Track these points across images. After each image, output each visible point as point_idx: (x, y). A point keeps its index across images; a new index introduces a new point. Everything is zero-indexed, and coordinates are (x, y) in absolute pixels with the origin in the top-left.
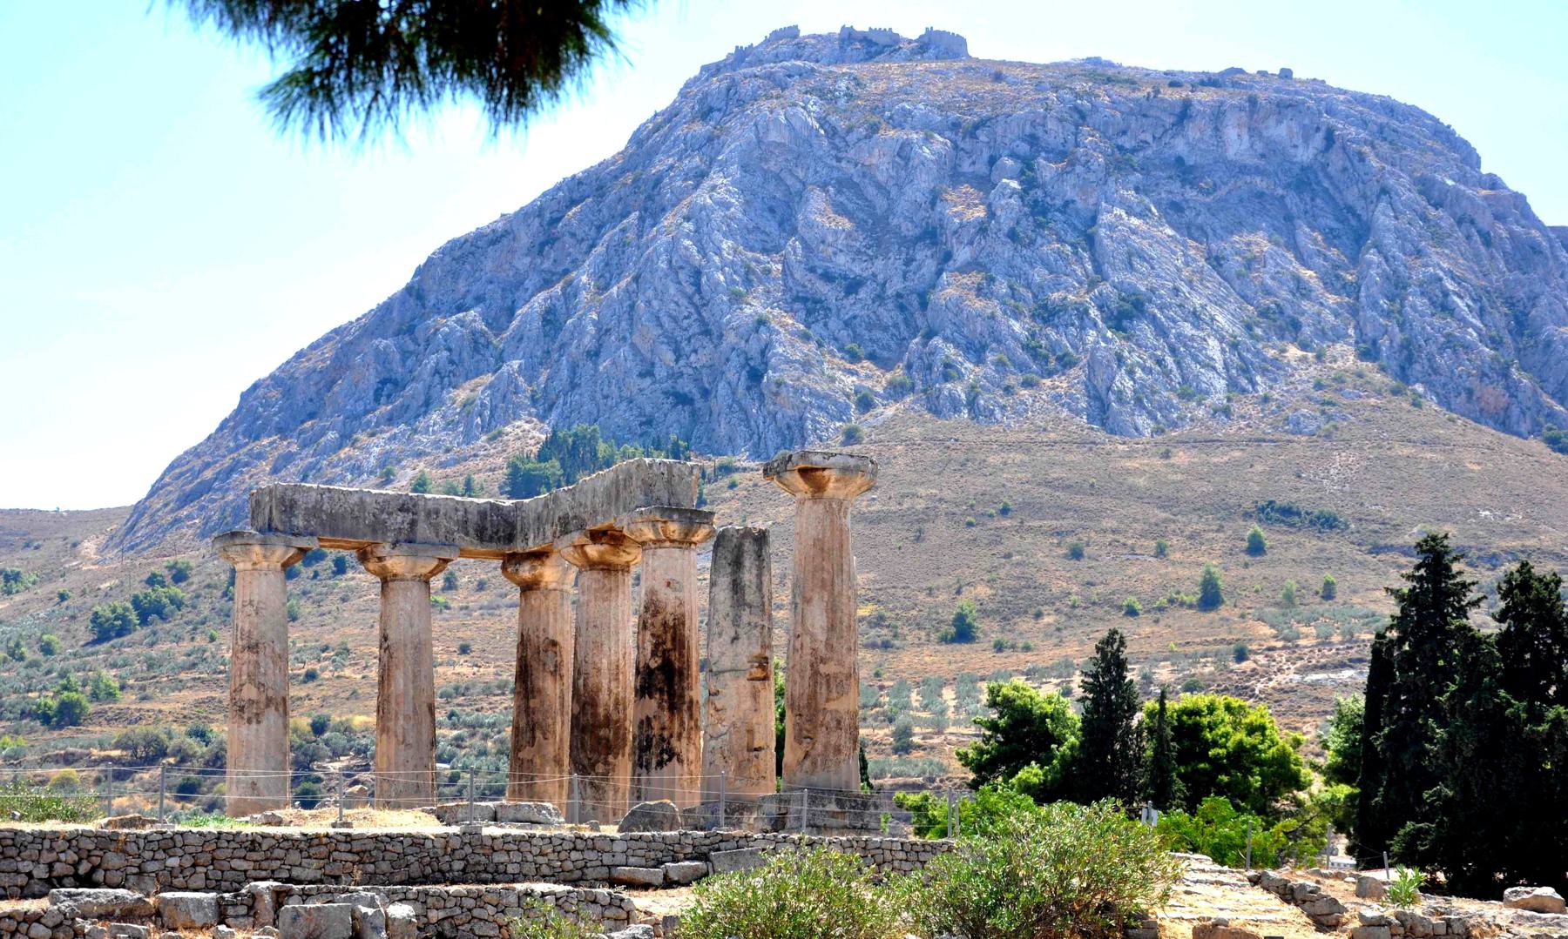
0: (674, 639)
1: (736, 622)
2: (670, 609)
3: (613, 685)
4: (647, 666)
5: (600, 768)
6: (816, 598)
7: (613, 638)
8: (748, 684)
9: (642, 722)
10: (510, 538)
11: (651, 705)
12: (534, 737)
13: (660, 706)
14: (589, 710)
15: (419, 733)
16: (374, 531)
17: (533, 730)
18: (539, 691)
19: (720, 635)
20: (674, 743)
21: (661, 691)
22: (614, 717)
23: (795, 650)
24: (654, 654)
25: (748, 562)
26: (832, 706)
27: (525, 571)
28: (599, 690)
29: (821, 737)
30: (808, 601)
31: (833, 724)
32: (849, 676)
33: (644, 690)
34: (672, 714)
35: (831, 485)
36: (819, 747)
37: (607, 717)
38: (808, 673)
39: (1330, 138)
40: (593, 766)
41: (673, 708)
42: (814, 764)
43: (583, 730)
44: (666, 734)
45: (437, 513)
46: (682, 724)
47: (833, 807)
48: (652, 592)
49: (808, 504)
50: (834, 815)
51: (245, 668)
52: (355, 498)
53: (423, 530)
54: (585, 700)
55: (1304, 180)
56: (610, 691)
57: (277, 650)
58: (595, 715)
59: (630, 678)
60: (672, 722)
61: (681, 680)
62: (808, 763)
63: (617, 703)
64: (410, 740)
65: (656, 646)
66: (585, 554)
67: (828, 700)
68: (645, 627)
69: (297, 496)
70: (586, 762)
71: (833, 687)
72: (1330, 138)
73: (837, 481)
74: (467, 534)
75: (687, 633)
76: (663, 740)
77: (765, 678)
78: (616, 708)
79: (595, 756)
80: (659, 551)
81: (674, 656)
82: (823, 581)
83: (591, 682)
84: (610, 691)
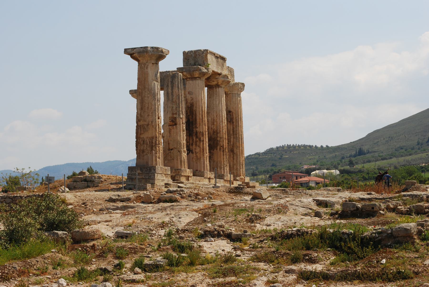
22: (213, 137)
31: (142, 142)
32: (148, 125)
46: (193, 140)
56: (211, 128)
60: (190, 140)
63: (214, 132)
78: (213, 134)
84: (211, 128)
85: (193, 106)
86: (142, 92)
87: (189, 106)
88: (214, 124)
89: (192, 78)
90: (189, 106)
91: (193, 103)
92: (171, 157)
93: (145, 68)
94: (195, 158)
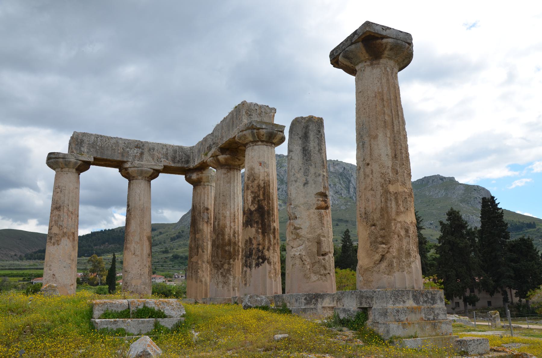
0: (264, 194)
1: (306, 173)
2: (261, 178)
3: (232, 224)
4: (250, 210)
5: (226, 266)
6: (381, 135)
7: (232, 202)
8: (316, 211)
9: (247, 241)
10: (188, 162)
11: (252, 231)
12: (198, 252)
13: (257, 231)
14: (221, 237)
15: (142, 250)
16: (123, 156)
17: (198, 248)
18: (200, 230)
19: (296, 181)
20: (266, 253)
21: (257, 223)
22: (233, 240)
23: (366, 176)
24: (253, 202)
25: (312, 135)
26: (399, 219)
27: (194, 176)
28: (225, 227)
29: (395, 243)
30: (376, 137)
31: (403, 233)
33: (248, 223)
34: (264, 236)
35: (386, 53)
36: (394, 252)
37: (230, 240)
38: (380, 191)
39: (344, 168)
40: (222, 265)
41: (263, 233)
42: (390, 265)
43: (218, 247)
44: (261, 247)
45: (154, 149)
47: (411, 303)
48: (252, 169)
49: (368, 69)
50: (412, 310)
51: (54, 218)
52: (114, 141)
53: (146, 156)
54: (219, 232)
55: (341, 174)
56: (231, 227)
57: (71, 209)
58: (223, 239)
59: (240, 218)
60: (264, 240)
61: (269, 217)
62: (384, 265)
63: (234, 233)
64: (138, 253)
65: (254, 198)
66: (218, 160)
67: (398, 213)
68: (248, 189)
69: (84, 138)
70: (219, 263)
71: (400, 202)
72: (344, 168)
73: (391, 49)
74: (167, 159)
75: (271, 191)
76: (259, 251)
77: (327, 208)
79: (224, 261)
80: (256, 147)
81: (265, 203)
82: (385, 122)
83: (221, 223)
84: (231, 227)
85: (269, 185)
86: (393, 122)
87: (262, 185)
88: (234, 221)
89: (267, 142)
90: (262, 185)
91: (269, 181)
92: (325, 269)
93: (394, 76)
94: (273, 271)
